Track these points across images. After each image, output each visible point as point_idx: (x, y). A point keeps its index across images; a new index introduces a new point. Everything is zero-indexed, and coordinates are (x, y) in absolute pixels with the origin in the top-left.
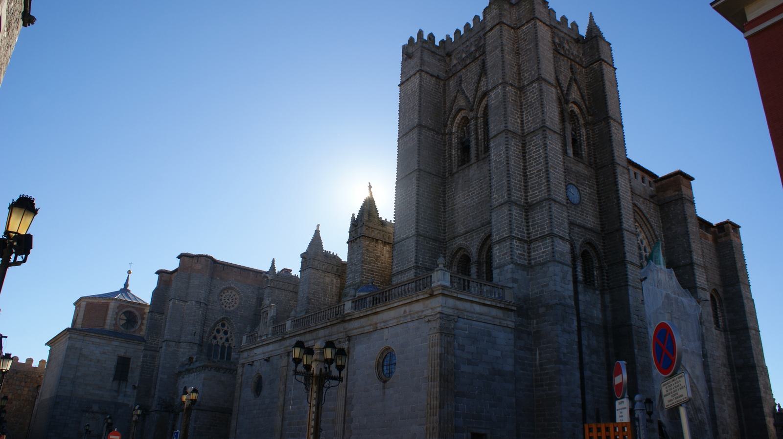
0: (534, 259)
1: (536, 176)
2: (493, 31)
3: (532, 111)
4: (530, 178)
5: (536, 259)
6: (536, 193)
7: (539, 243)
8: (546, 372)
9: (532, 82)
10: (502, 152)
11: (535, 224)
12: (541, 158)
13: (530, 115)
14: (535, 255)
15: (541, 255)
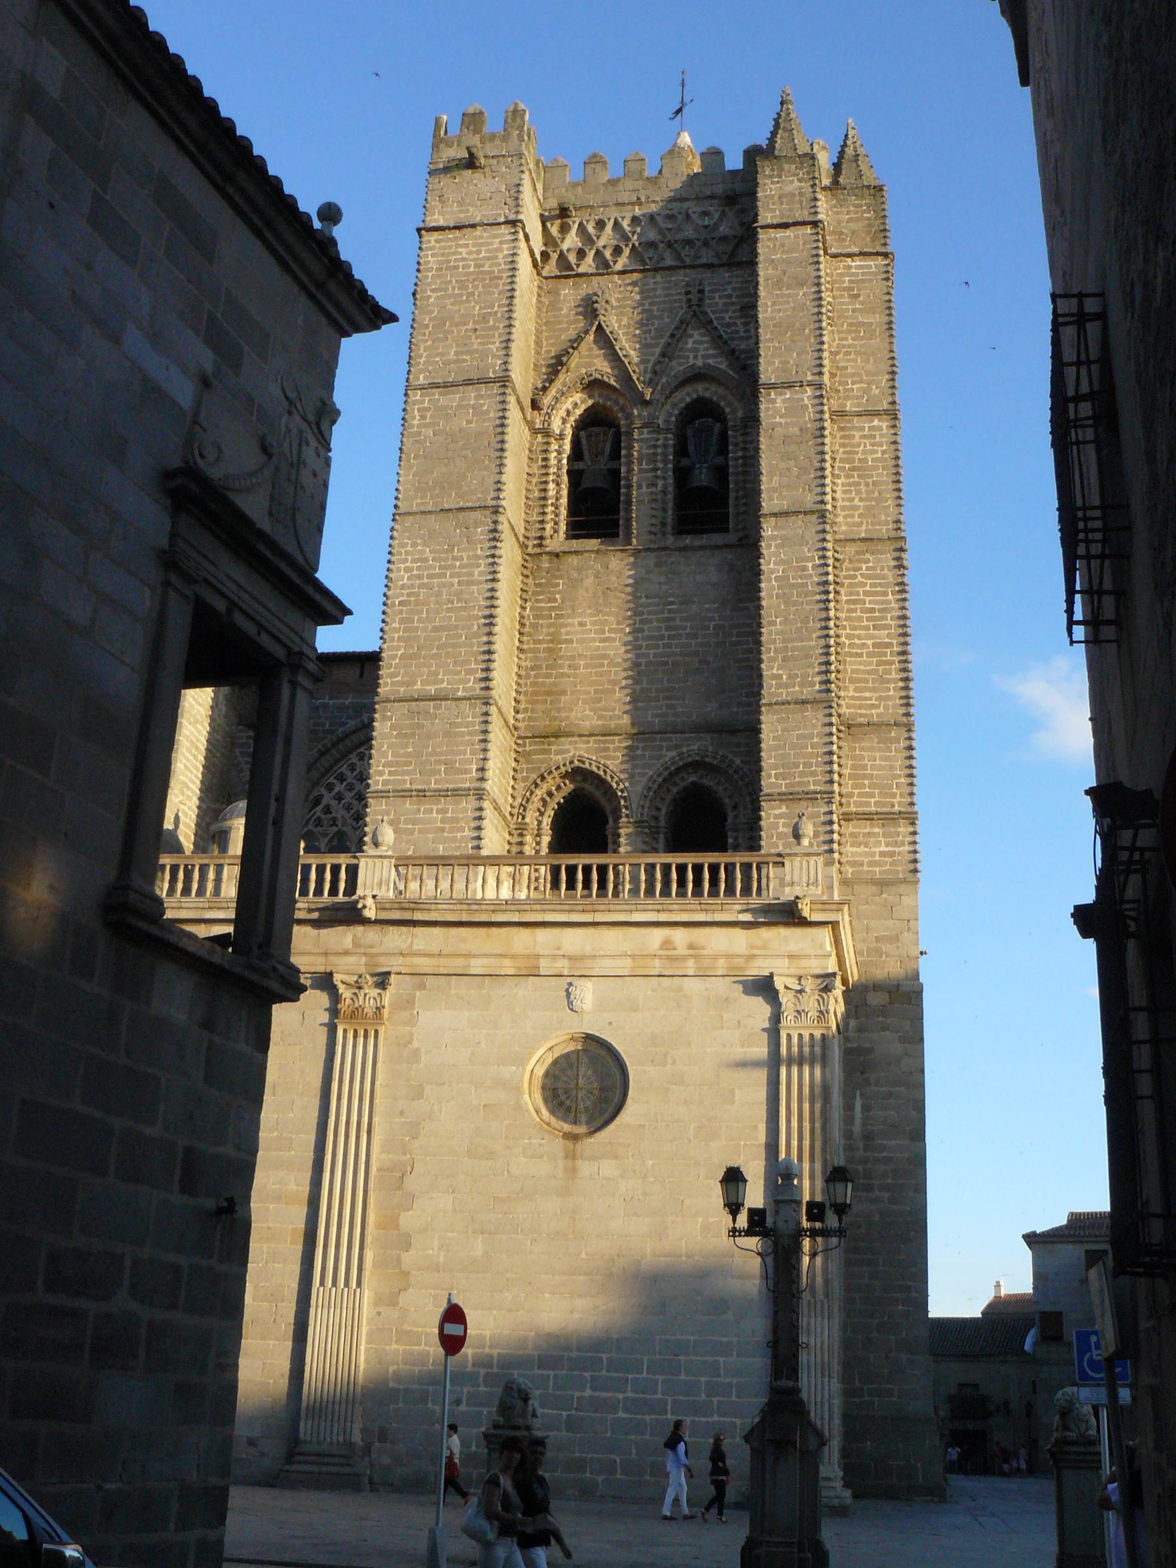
0: (853, 864)
1: (869, 655)
2: (788, 232)
3: (867, 485)
4: (851, 655)
5: (862, 864)
6: (870, 699)
7: (872, 826)
8: (885, 1154)
9: (876, 414)
10: (810, 565)
11: (864, 777)
12: (889, 615)
13: (858, 492)
14: (854, 854)
15: (877, 858)
